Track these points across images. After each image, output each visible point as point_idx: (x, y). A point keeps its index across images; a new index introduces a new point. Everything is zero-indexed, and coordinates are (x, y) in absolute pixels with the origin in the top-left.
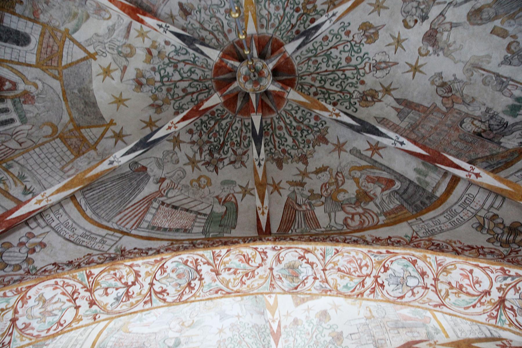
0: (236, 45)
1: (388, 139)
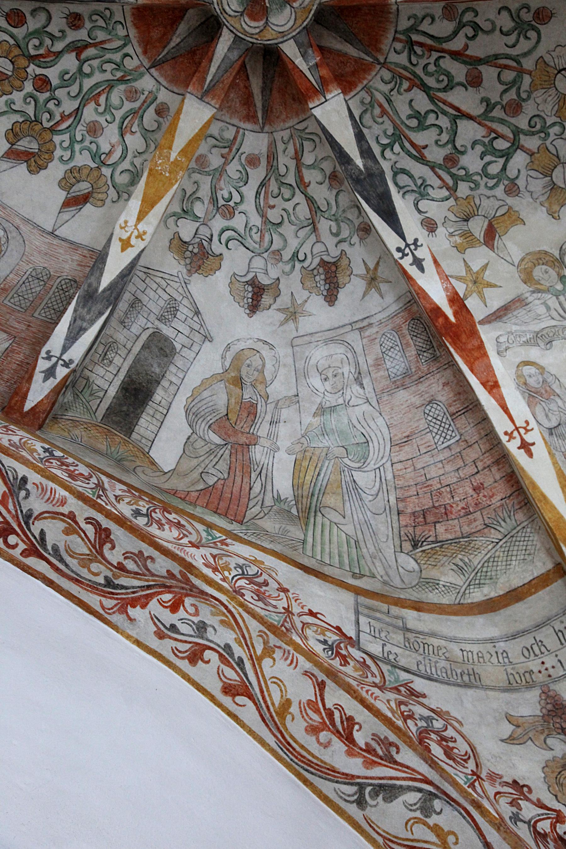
0: (260, 115)
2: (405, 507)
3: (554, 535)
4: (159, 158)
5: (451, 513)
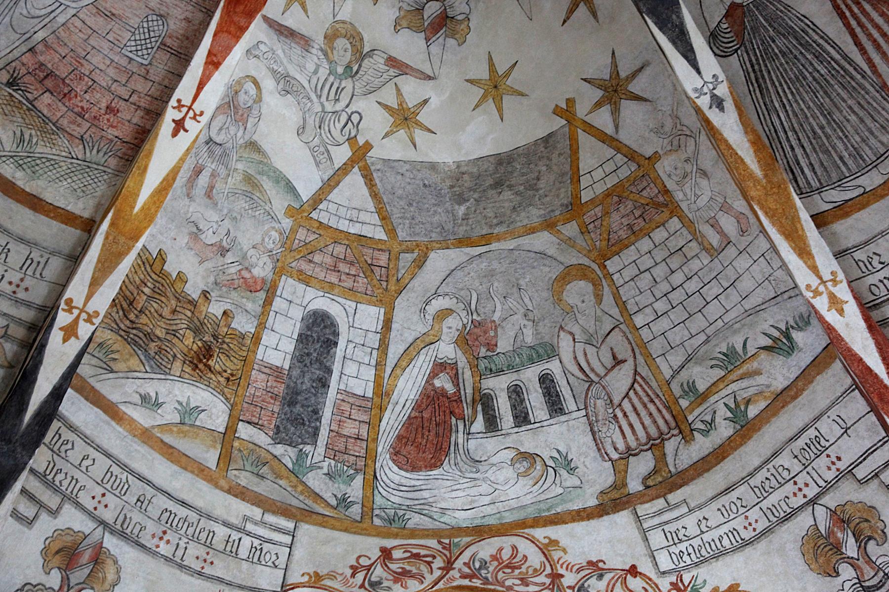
2: (42, 53)
3: (117, 199)
5: (70, 99)
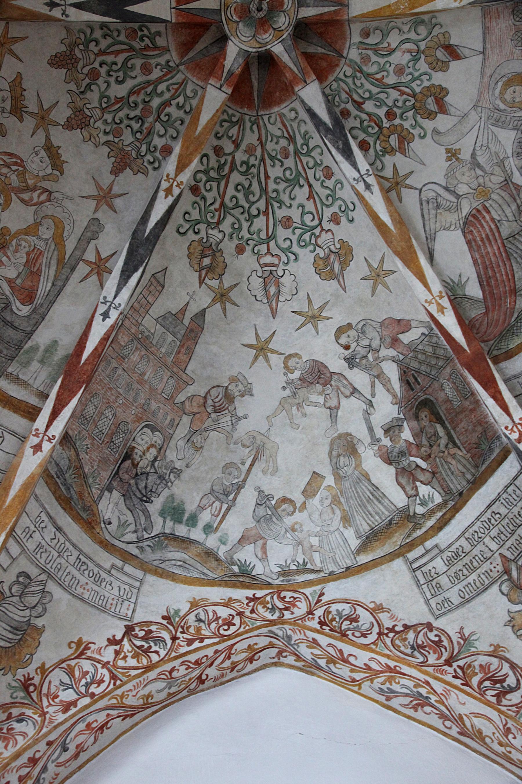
1: (114, 289)
4: (400, 9)
